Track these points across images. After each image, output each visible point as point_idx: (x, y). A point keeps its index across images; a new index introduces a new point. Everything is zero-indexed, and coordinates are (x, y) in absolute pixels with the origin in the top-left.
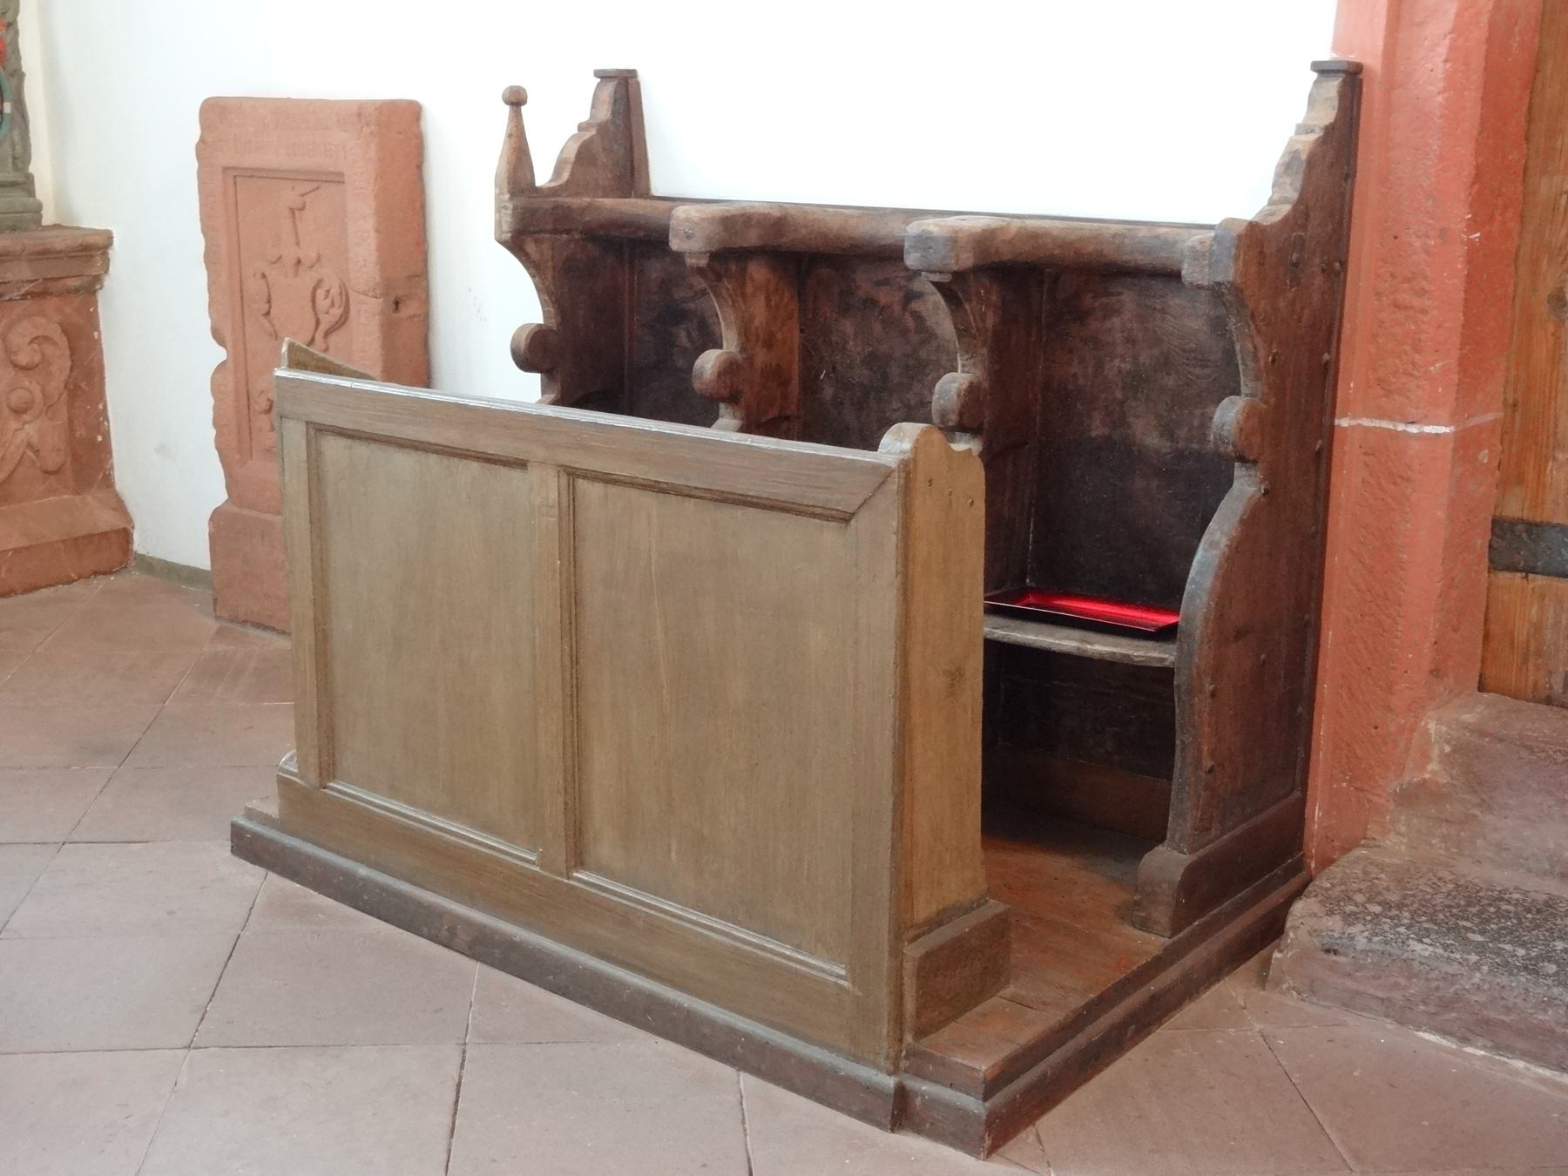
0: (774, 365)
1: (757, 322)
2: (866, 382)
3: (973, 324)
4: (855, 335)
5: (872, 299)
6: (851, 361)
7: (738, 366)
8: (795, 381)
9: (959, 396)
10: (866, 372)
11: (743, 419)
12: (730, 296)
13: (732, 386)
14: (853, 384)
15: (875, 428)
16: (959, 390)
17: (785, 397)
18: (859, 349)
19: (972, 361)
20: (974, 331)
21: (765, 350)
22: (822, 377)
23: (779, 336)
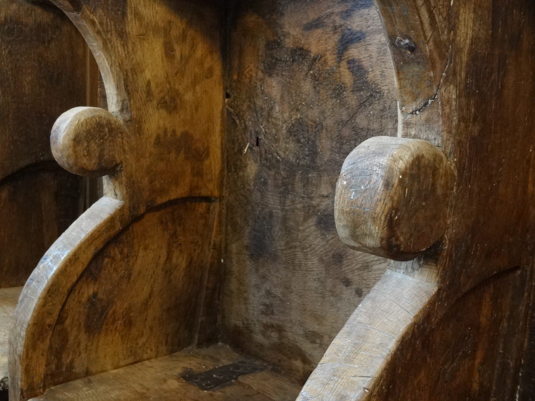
0: (179, 132)
1: (148, 75)
2: (292, 159)
3: (429, 34)
4: (282, 97)
5: (301, 49)
6: (277, 131)
7: (111, 130)
8: (216, 152)
9: (387, 185)
10: (292, 145)
11: (123, 199)
12: (99, 33)
13: (101, 156)
14: (278, 161)
15: (301, 219)
16: (390, 170)
17: (198, 173)
18: (286, 115)
19: (424, 115)
20: (428, 48)
21: (163, 112)
22: (246, 150)
23: (188, 97)
